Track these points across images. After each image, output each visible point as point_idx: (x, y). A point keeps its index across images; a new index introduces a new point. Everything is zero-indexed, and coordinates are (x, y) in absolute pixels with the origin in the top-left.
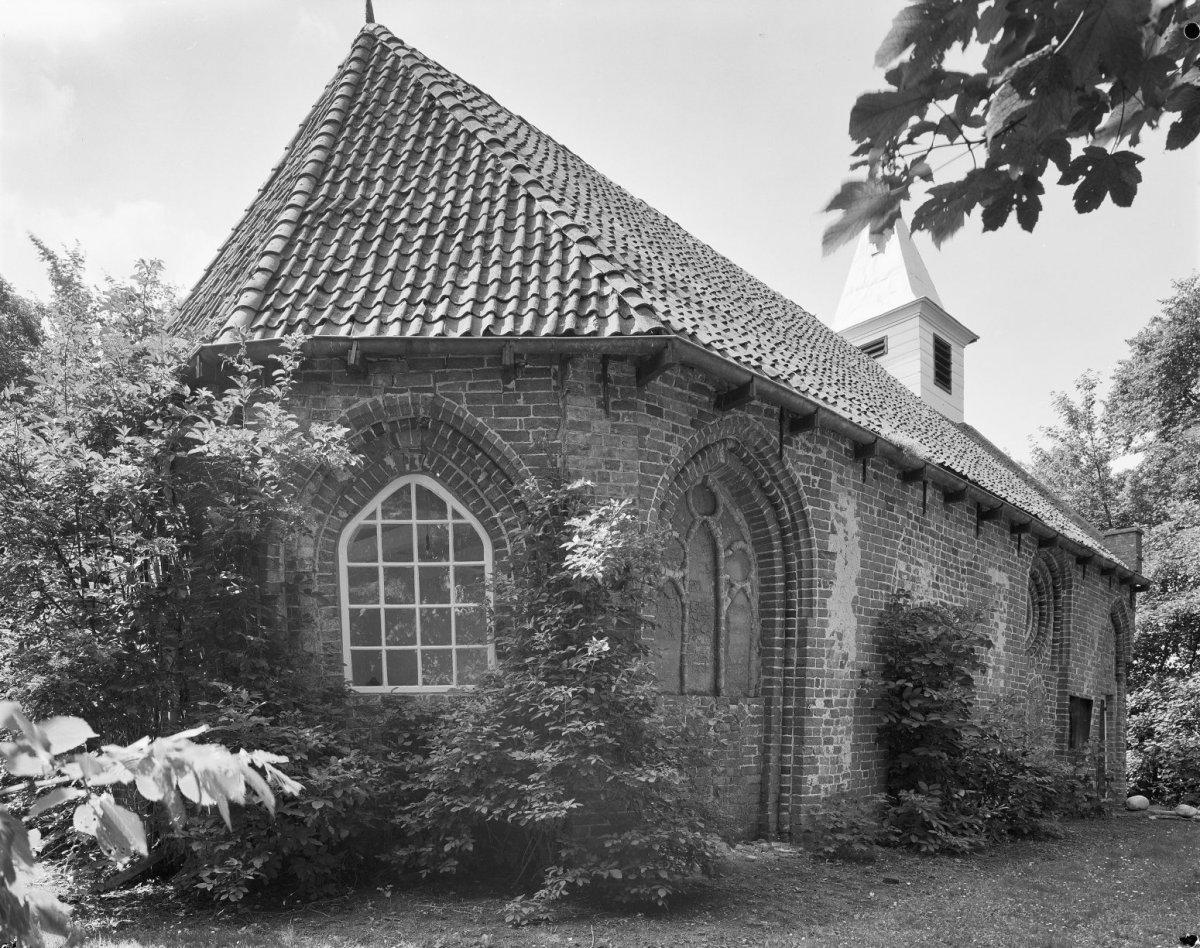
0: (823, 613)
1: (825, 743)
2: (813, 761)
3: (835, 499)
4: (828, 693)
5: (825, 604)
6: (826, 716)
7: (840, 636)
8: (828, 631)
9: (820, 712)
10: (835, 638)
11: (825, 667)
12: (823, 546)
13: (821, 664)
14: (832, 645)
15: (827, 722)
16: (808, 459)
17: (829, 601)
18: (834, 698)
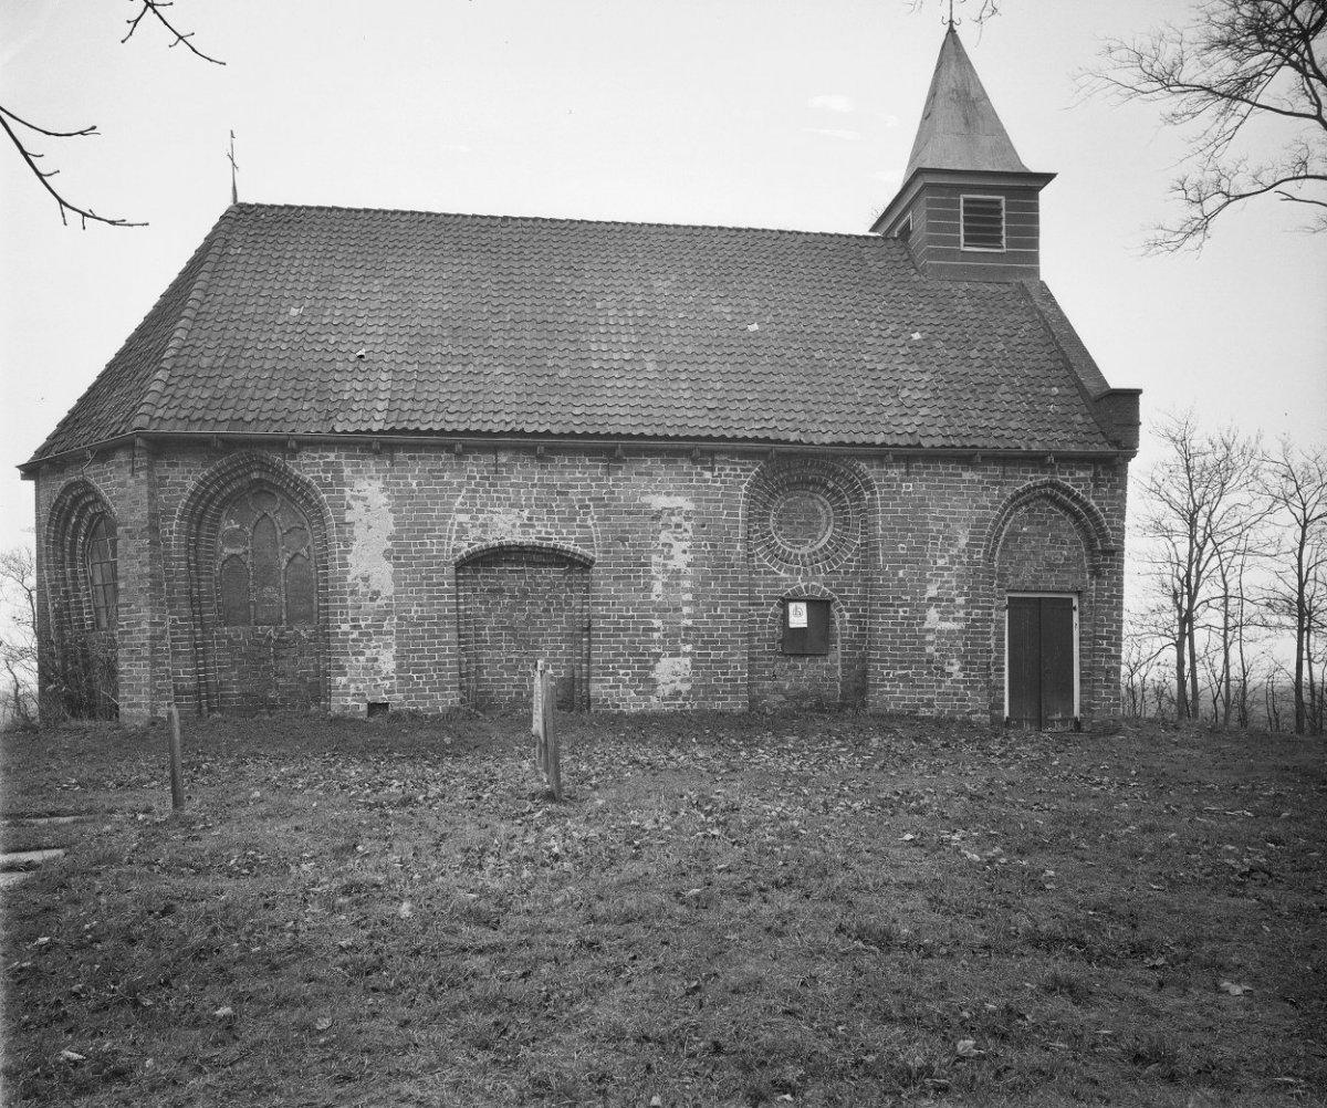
0: (346, 565)
1: (353, 654)
2: (341, 667)
3: (351, 486)
4: (353, 620)
5: (344, 559)
6: (355, 635)
7: (366, 580)
8: (349, 578)
9: (346, 633)
10: (359, 581)
11: (349, 603)
12: (342, 523)
13: (345, 600)
14: (357, 585)
15: (353, 640)
16: (317, 465)
17: (348, 557)
18: (363, 624)
